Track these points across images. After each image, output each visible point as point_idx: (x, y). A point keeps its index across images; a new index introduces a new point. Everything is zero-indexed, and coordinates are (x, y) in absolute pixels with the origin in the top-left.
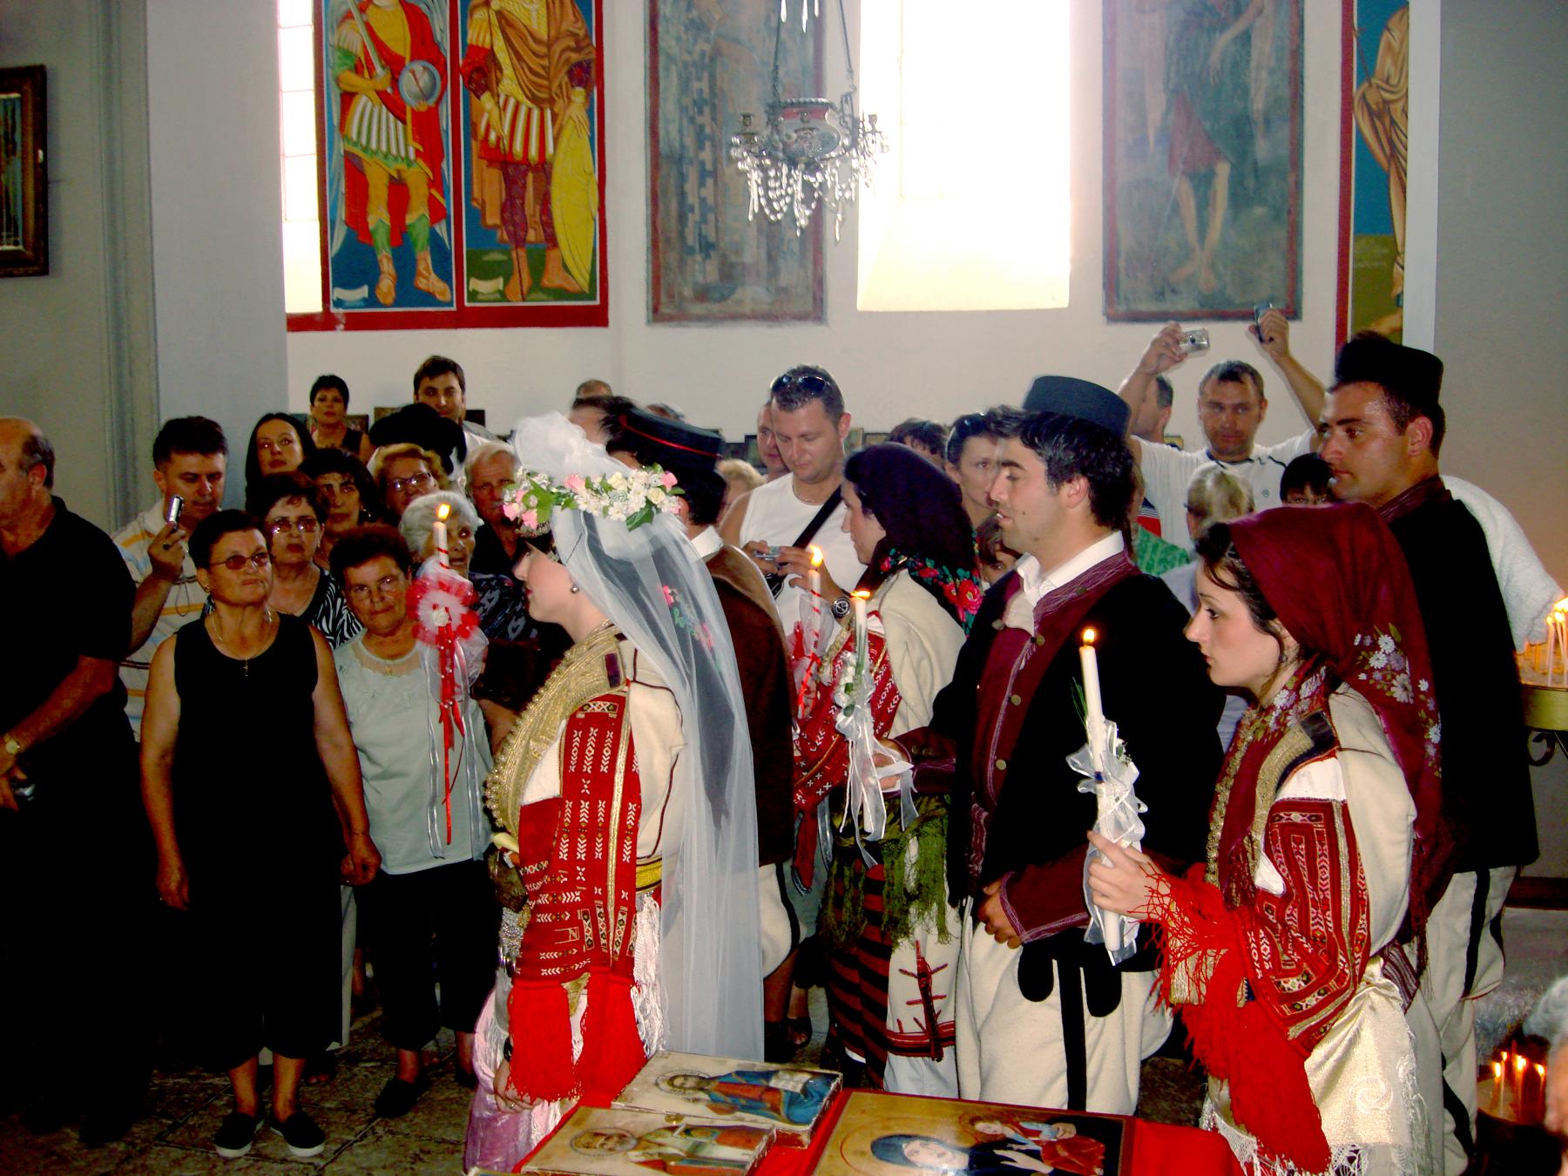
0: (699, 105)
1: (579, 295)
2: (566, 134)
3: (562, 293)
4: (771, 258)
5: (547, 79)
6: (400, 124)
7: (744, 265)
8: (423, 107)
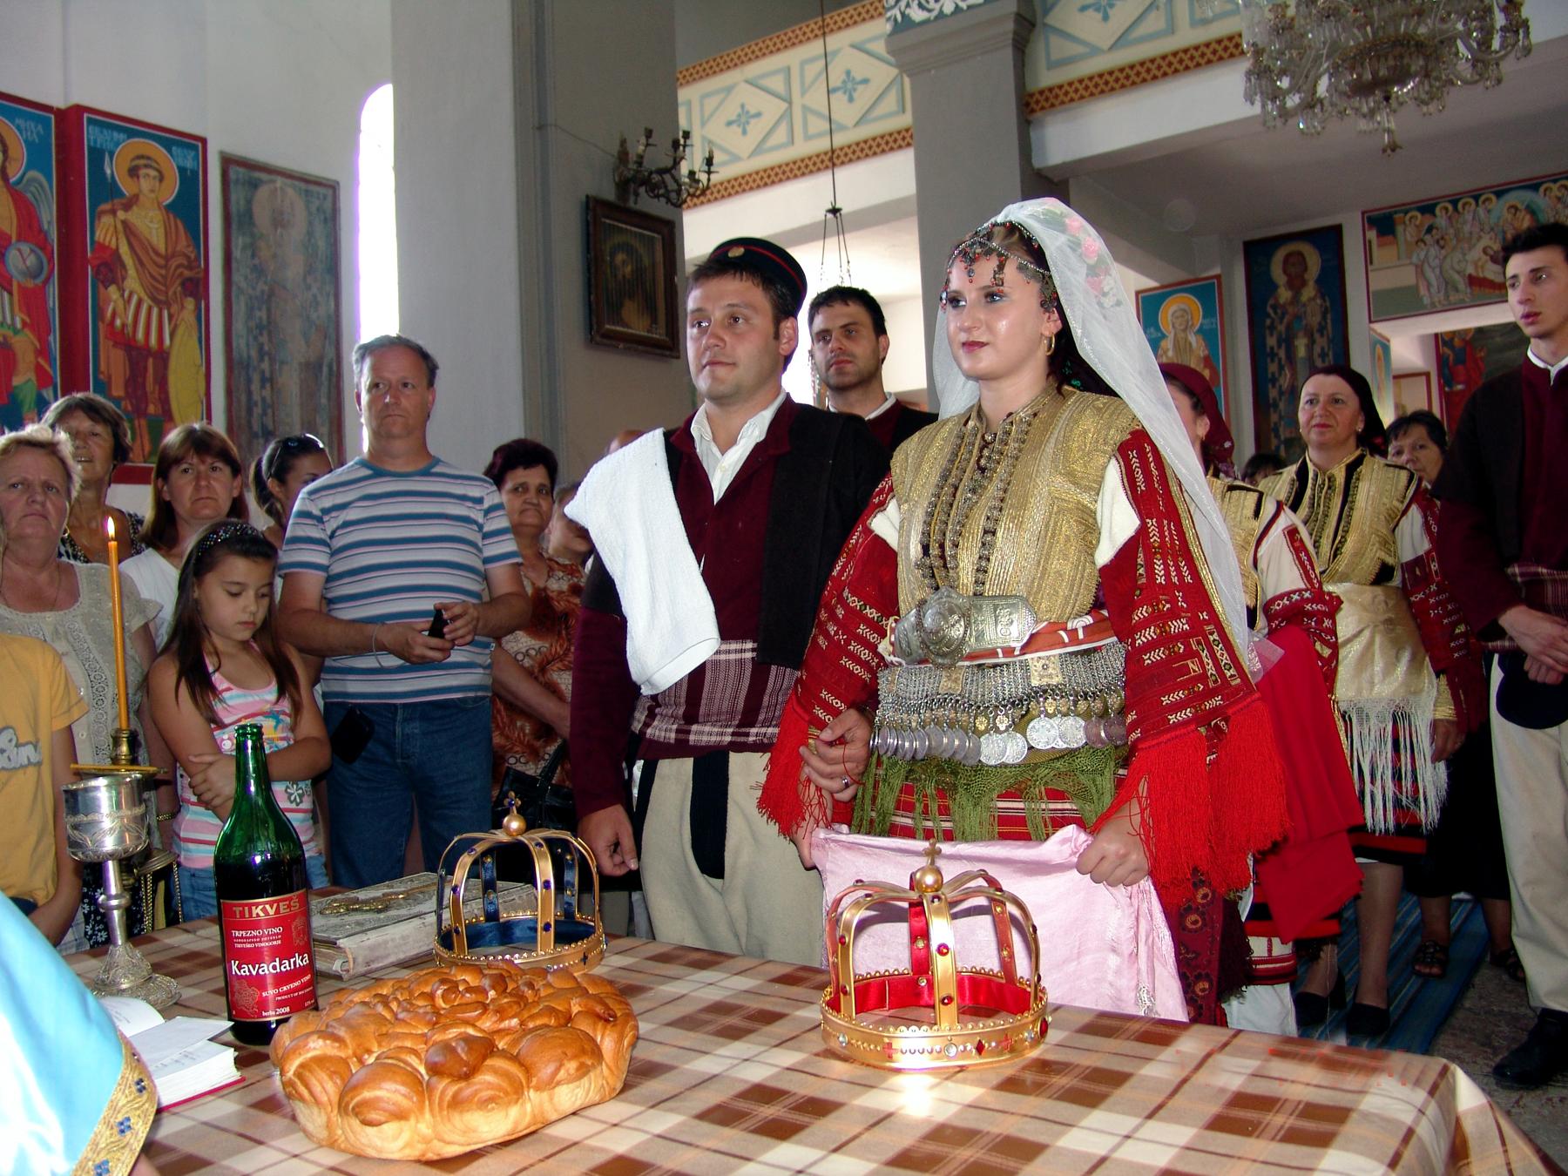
0: (260, 327)
2: (180, 331)
5: (165, 285)
6: (6, 295)
8: (30, 284)
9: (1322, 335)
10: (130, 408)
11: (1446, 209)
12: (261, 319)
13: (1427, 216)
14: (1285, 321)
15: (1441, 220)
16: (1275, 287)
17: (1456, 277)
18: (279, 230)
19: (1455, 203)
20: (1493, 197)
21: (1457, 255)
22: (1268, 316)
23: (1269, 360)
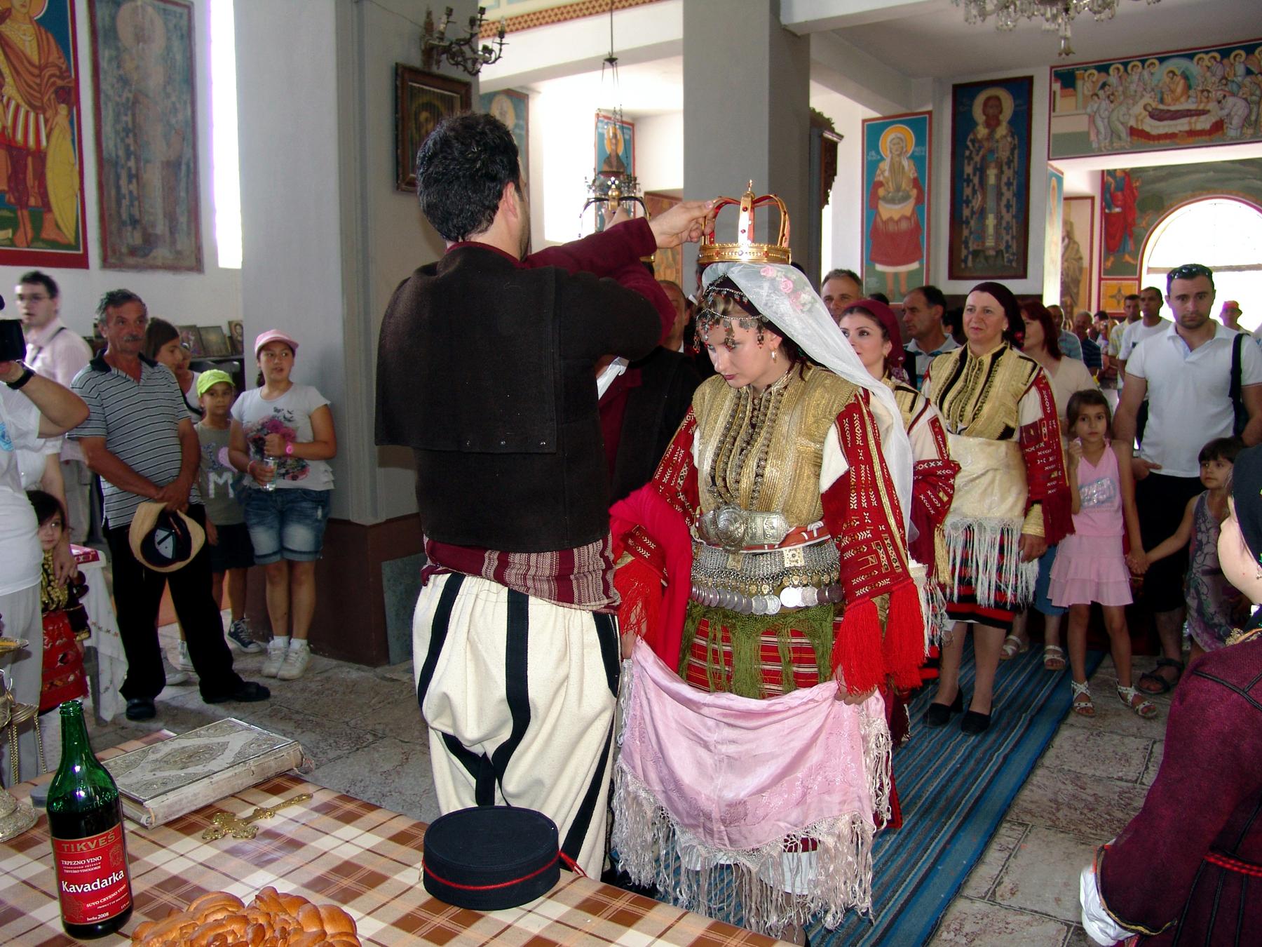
0: (127, 131)
1: (68, 246)
2: (56, 133)
3: (54, 244)
4: (172, 233)
7: (157, 236)
9: (1009, 168)
10: (12, 200)
11: (1118, 69)
12: (127, 123)
13: (1103, 74)
14: (981, 153)
15: (1113, 79)
16: (975, 124)
17: (1120, 127)
18: (141, 44)
19: (1125, 65)
20: (1156, 62)
21: (1124, 109)
22: (968, 148)
23: (965, 184)
